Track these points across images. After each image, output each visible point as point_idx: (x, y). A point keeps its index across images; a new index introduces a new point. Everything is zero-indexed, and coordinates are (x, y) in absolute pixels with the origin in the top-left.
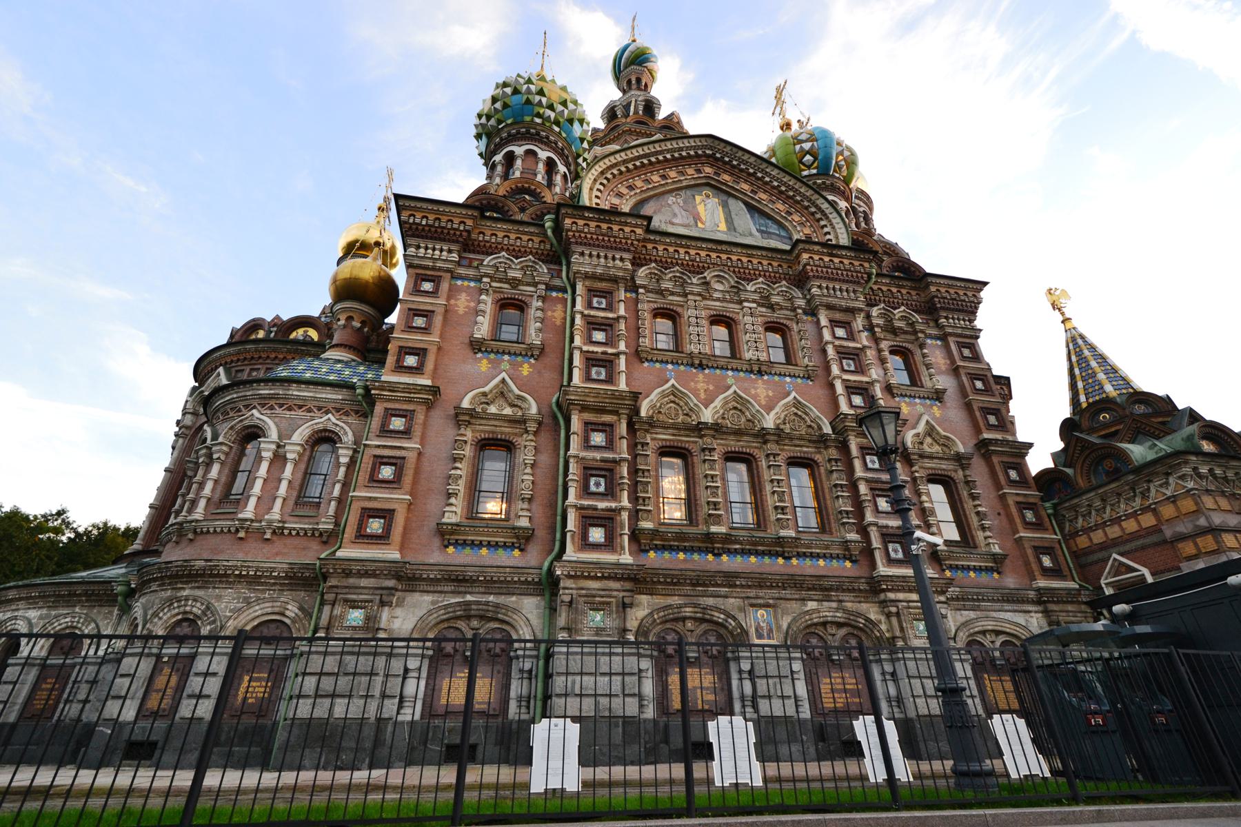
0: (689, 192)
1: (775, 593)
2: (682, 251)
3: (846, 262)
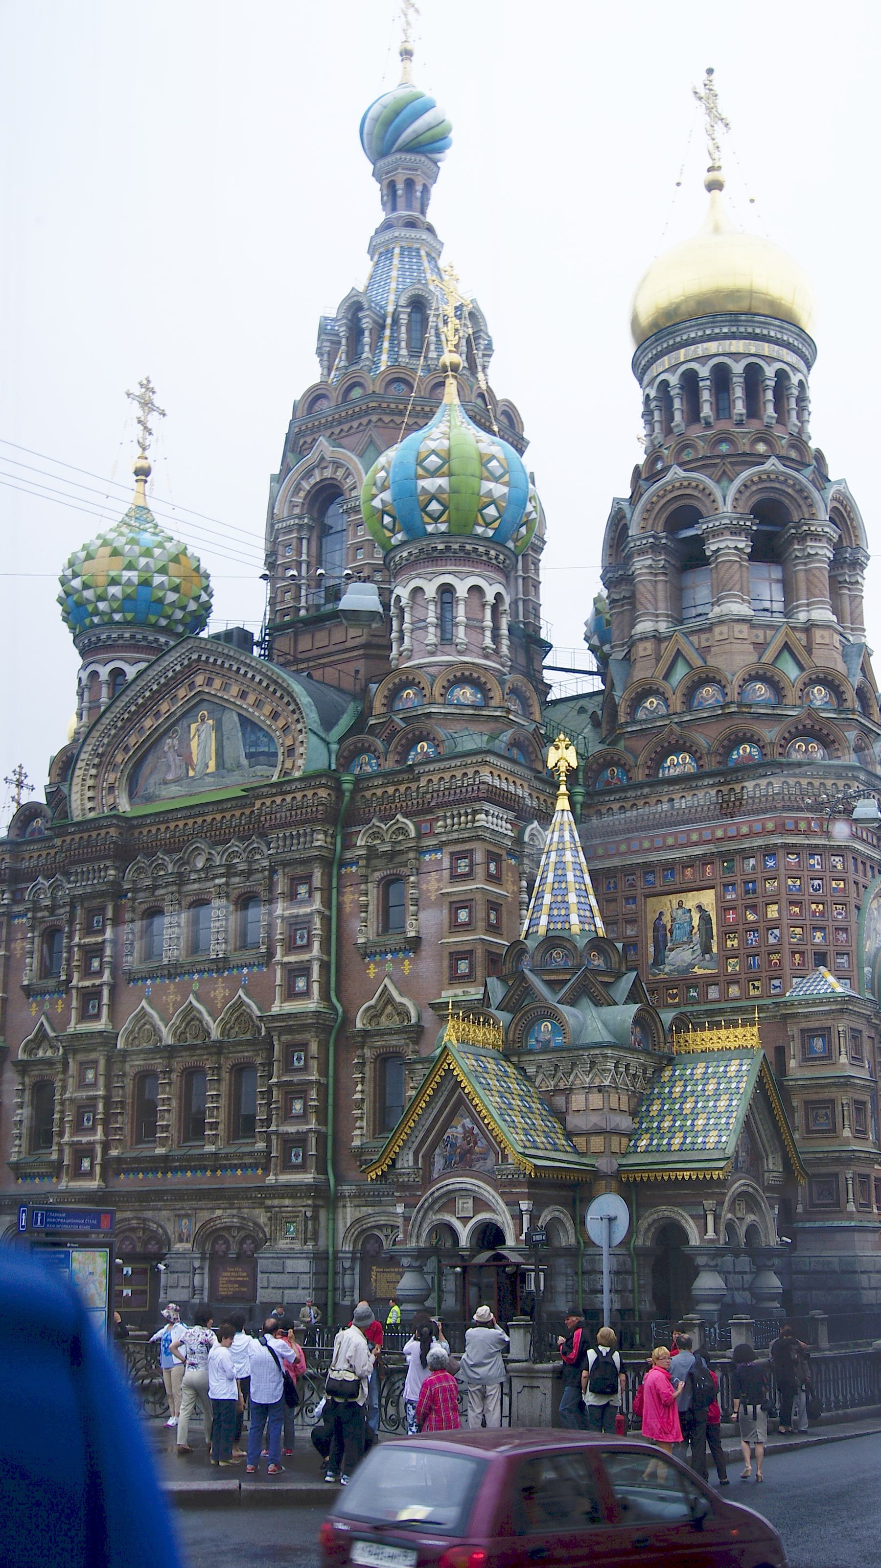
0: (185, 722)
1: (195, 1204)
2: (163, 828)
3: (299, 796)
